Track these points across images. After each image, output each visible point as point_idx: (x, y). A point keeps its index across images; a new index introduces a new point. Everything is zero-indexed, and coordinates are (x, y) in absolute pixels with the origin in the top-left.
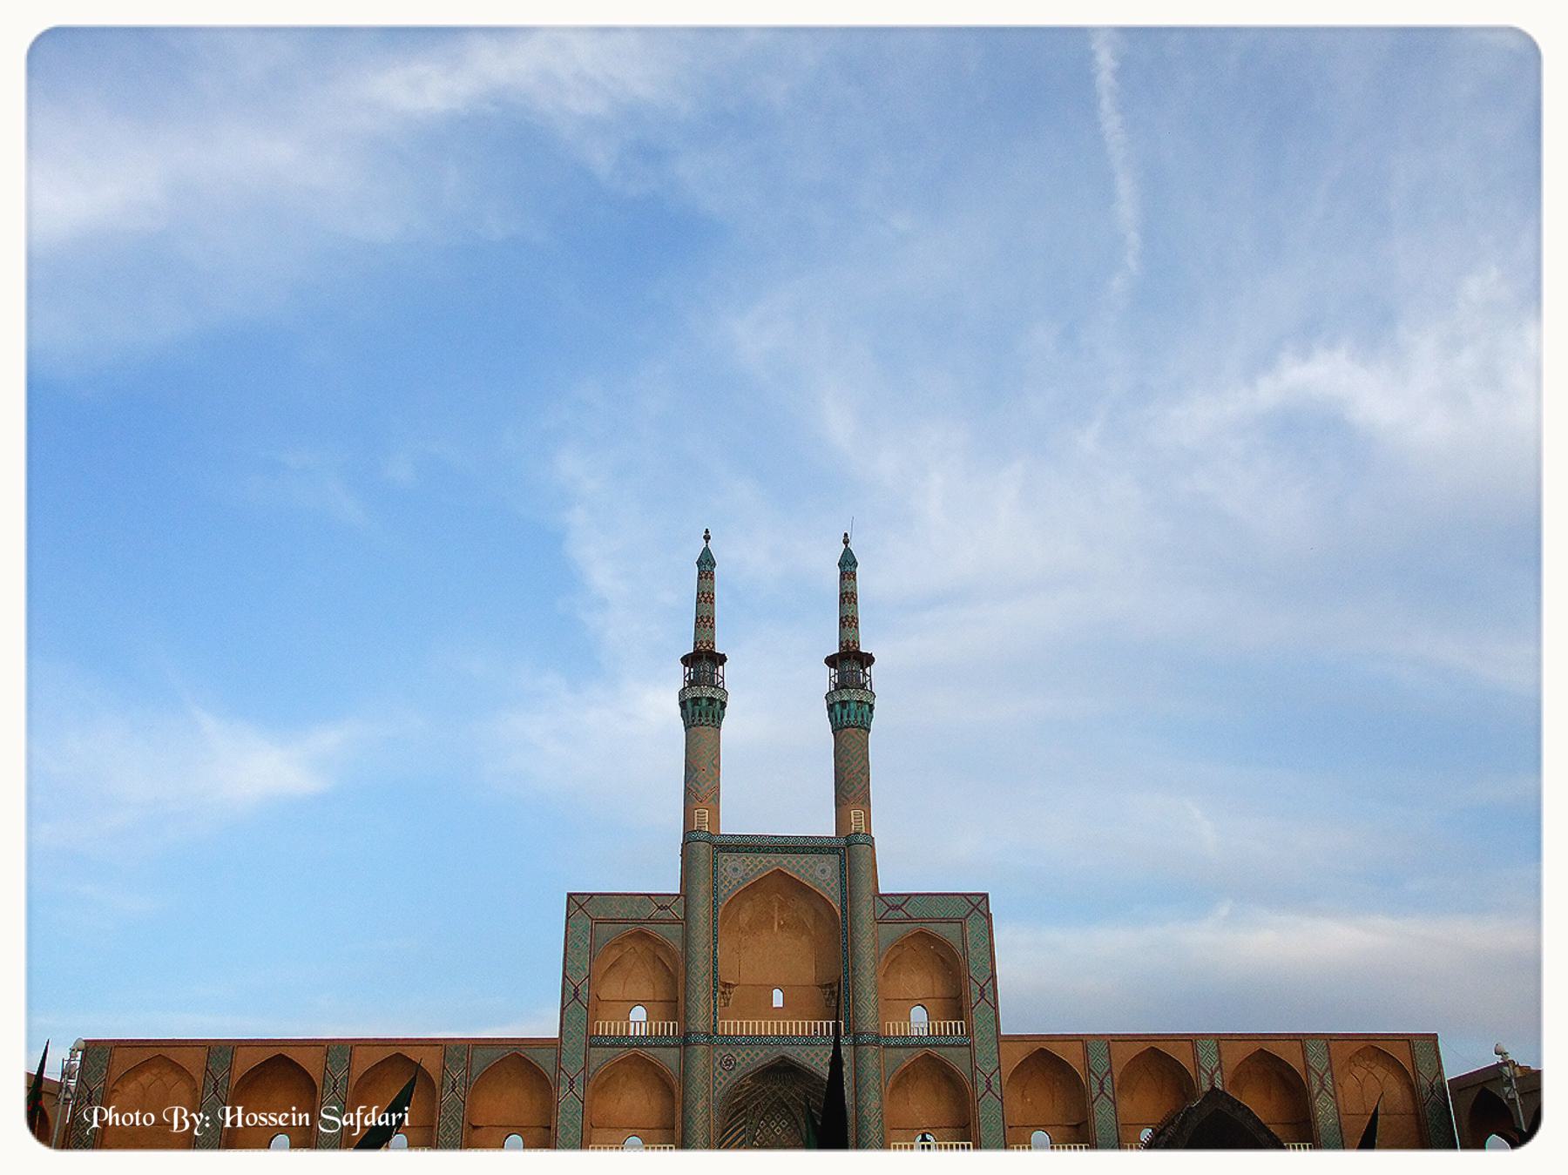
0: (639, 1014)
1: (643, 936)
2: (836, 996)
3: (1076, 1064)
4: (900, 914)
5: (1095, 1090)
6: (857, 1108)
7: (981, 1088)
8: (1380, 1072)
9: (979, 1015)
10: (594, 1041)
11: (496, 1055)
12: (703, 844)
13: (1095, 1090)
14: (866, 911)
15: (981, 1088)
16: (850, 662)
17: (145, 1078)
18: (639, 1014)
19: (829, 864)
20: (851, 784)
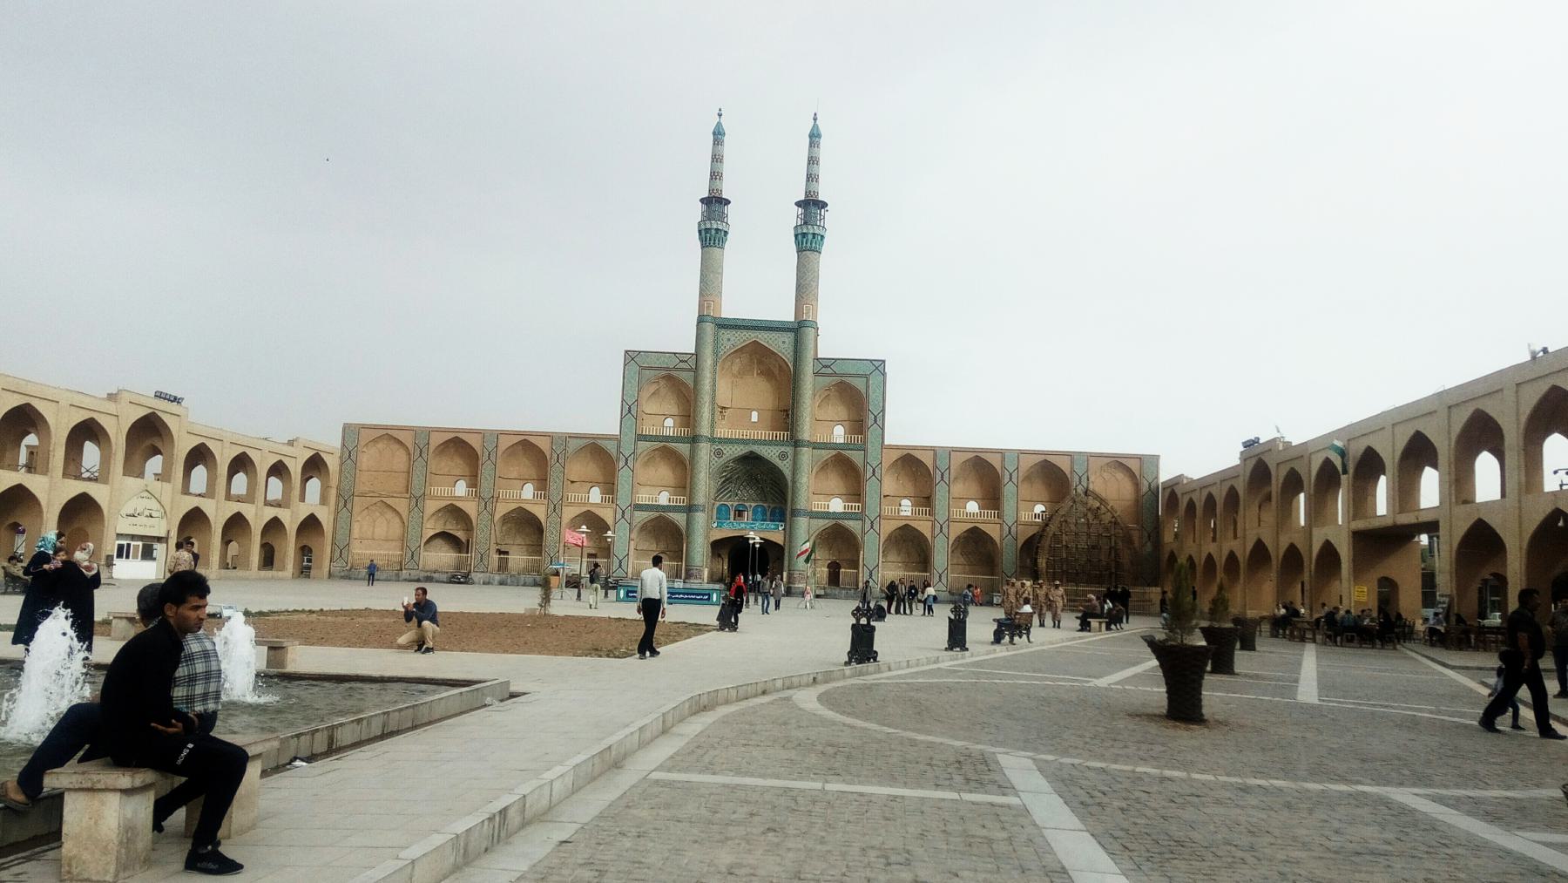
0: (669, 422)
1: (669, 378)
2: (786, 417)
3: (929, 463)
4: (829, 371)
5: (938, 478)
6: (794, 482)
7: (869, 473)
9: (872, 434)
10: (642, 437)
11: (582, 442)
12: (711, 323)
13: (938, 478)
14: (808, 369)
15: (869, 473)
17: (380, 445)
18: (669, 422)
19: (788, 338)
20: (805, 288)
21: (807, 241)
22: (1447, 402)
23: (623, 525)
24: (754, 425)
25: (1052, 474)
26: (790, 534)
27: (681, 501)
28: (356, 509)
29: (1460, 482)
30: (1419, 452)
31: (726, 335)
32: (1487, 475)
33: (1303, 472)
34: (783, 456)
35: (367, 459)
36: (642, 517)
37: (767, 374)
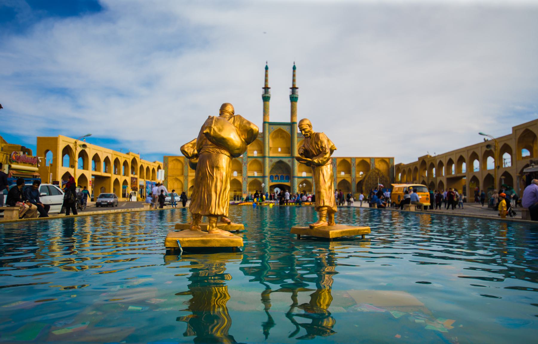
8: (383, 163)
16: (294, 88)
17: (174, 162)
19: (289, 127)
20: (293, 112)
21: (293, 99)
22: (467, 149)
23: (245, 182)
24: (279, 153)
25: (365, 164)
26: (292, 183)
27: (260, 175)
28: (169, 180)
29: (470, 166)
30: (461, 160)
31: (271, 126)
32: (476, 164)
33: (434, 163)
34: (289, 161)
35: (171, 165)
36: (250, 180)
37: (283, 137)
